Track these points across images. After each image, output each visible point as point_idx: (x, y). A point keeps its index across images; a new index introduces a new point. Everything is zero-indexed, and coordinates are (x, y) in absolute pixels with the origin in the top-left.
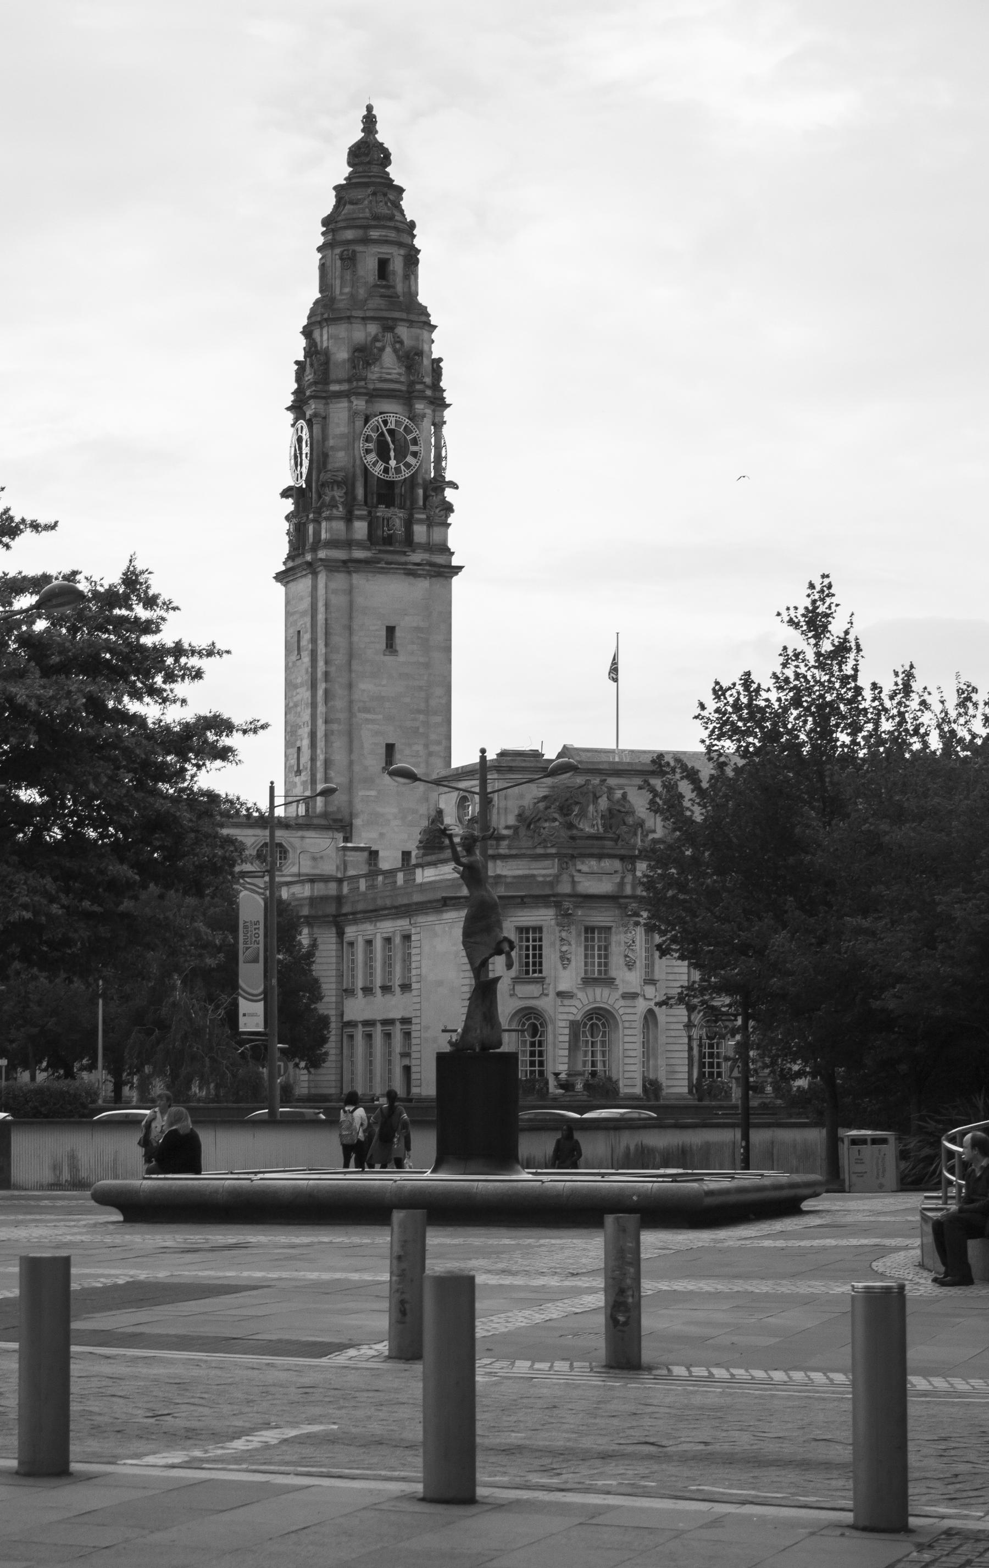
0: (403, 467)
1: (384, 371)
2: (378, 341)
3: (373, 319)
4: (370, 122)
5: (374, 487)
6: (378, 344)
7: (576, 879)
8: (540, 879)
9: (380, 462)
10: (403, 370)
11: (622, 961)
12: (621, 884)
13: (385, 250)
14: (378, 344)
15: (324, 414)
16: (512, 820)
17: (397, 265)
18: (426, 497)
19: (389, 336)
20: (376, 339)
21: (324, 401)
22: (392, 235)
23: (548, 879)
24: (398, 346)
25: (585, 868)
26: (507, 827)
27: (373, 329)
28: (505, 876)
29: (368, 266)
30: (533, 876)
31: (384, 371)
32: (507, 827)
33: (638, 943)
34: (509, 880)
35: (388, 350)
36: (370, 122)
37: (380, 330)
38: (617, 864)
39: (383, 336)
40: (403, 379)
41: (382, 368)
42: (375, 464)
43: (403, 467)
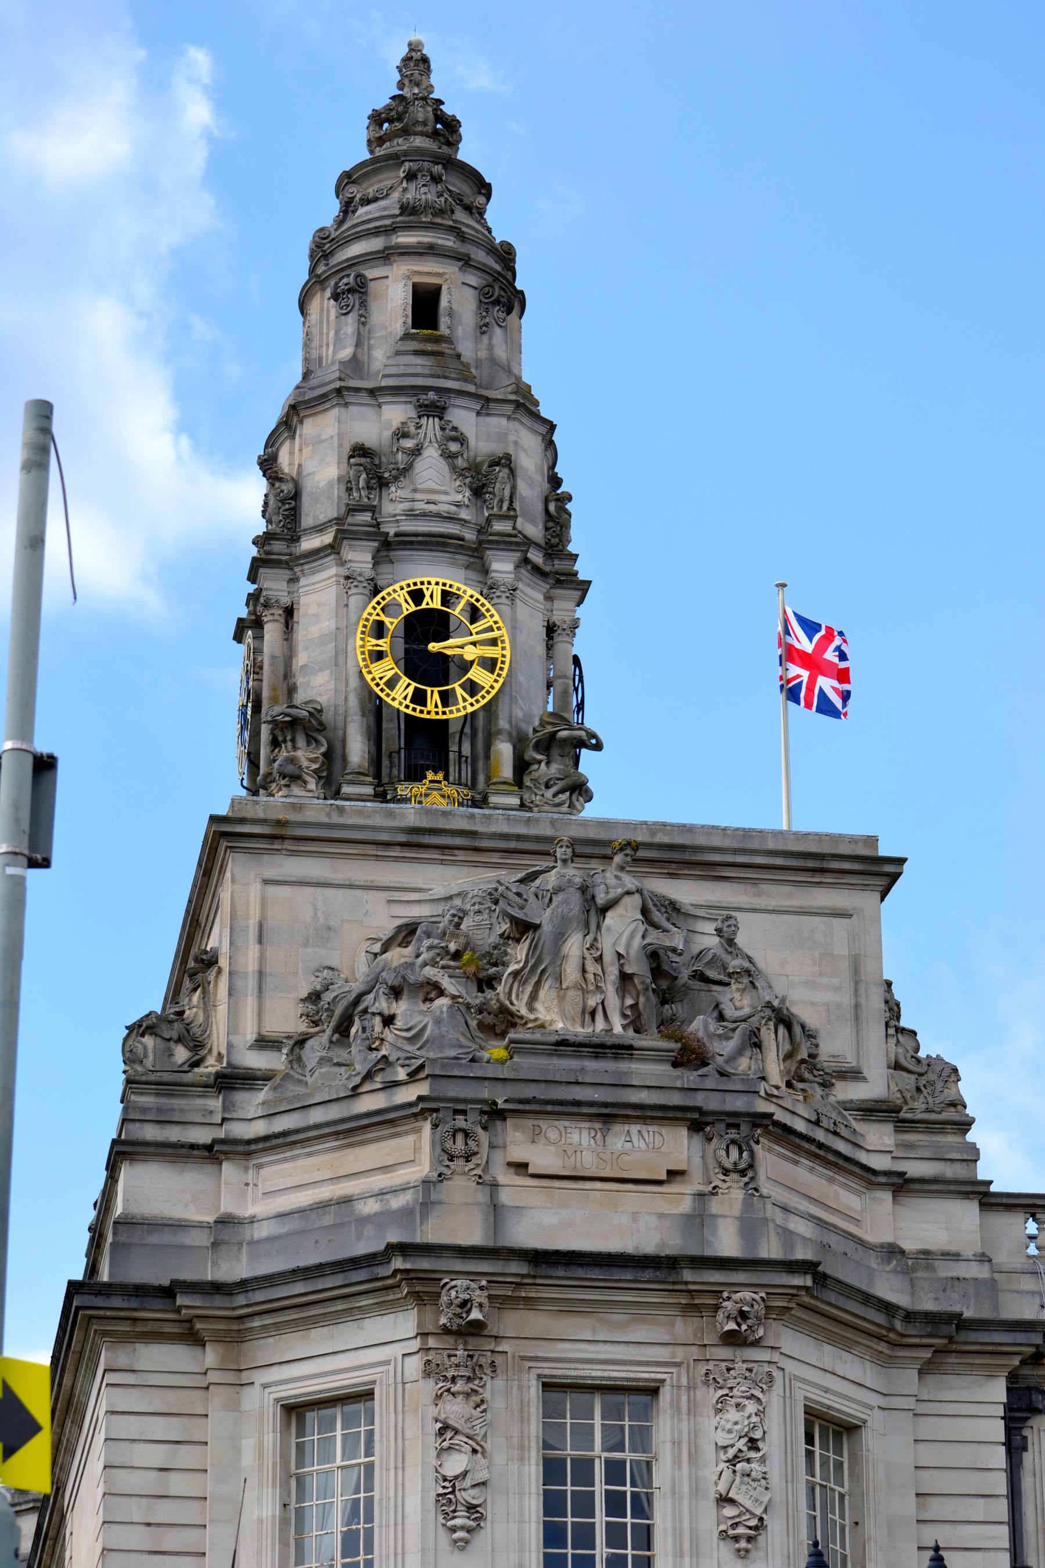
0: (459, 692)
1: (418, 496)
2: (406, 435)
3: (397, 391)
4: (416, 63)
5: (393, 736)
6: (409, 444)
7: (505, 1197)
8: (370, 1207)
9: (405, 680)
10: (465, 496)
11: (709, 1521)
12: (698, 1220)
13: (430, 270)
14: (409, 444)
15: (285, 600)
16: (286, 1018)
17: (459, 301)
18: (521, 766)
19: (431, 426)
20: (402, 434)
21: (286, 574)
22: (448, 242)
23: (396, 1203)
24: (454, 447)
25: (543, 1157)
26: (263, 1043)
27: (397, 413)
28: (252, 1220)
29: (393, 295)
30: (347, 1201)
31: (418, 496)
32: (263, 1043)
33: (772, 1447)
34: (262, 1231)
35: (431, 454)
36: (416, 63)
37: (413, 414)
38: (677, 1146)
39: (418, 427)
40: (464, 514)
41: (415, 490)
42: (391, 684)
43: (459, 692)
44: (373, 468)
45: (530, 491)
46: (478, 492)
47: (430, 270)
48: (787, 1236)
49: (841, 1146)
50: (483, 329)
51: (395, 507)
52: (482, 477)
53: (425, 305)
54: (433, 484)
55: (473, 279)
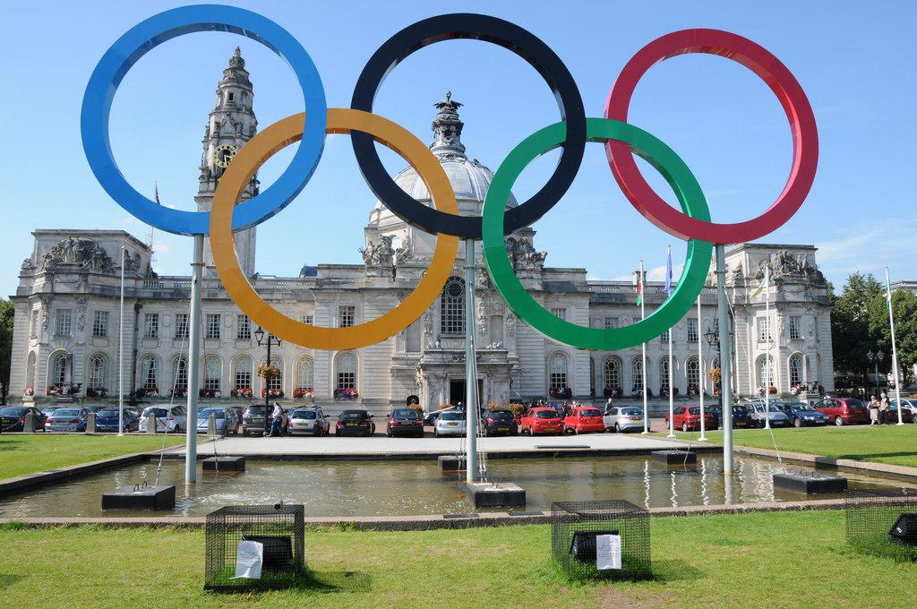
4: (238, 50)
13: (231, 90)
22: (236, 84)
38: (76, 277)
44: (218, 125)
45: (246, 127)
46: (236, 128)
47: (231, 90)
48: (94, 289)
49: (111, 274)
50: (242, 99)
51: (222, 131)
52: (236, 125)
53: (231, 96)
54: (229, 128)
55: (240, 90)
